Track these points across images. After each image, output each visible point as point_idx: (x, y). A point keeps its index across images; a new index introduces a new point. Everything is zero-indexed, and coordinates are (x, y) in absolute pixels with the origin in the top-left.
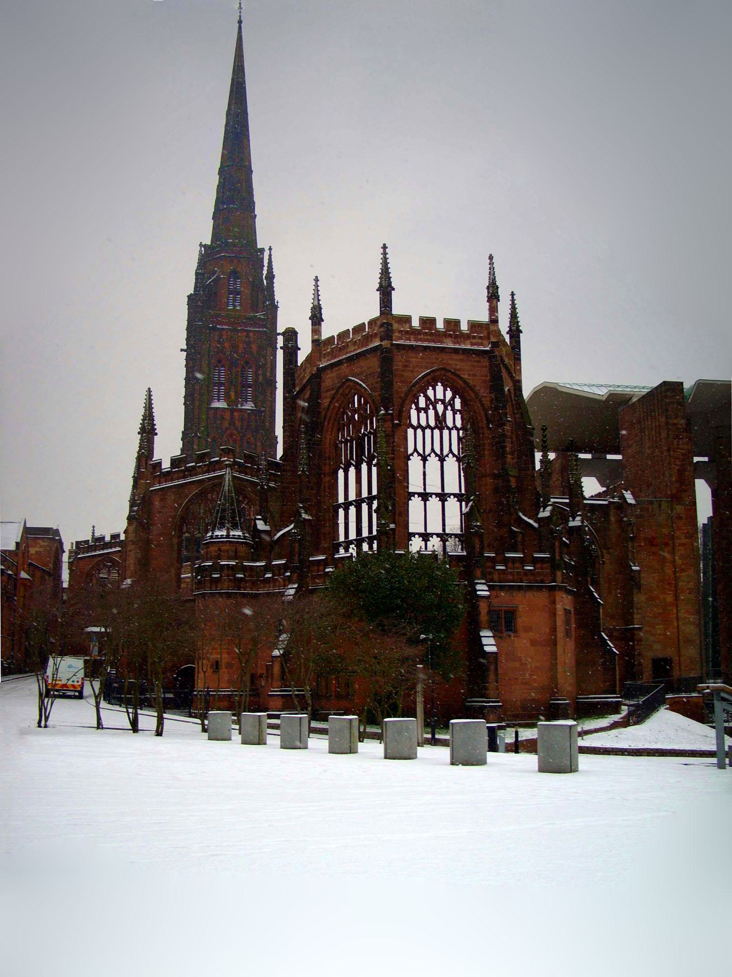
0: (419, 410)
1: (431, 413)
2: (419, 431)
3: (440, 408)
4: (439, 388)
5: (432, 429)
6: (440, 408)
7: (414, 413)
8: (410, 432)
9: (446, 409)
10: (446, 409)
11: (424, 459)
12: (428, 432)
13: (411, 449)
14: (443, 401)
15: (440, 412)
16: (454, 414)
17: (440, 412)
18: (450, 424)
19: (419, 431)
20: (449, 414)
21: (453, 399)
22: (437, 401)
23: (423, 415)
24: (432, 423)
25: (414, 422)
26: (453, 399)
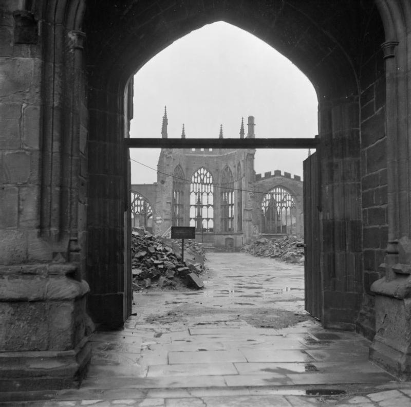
0: (195, 177)
1: (199, 178)
2: (195, 185)
3: (202, 176)
4: (202, 170)
5: (199, 184)
6: (202, 176)
7: (193, 178)
8: (192, 185)
9: (204, 177)
10: (204, 177)
11: (196, 194)
12: (197, 185)
13: (191, 190)
14: (203, 174)
15: (202, 178)
16: (207, 178)
17: (202, 178)
18: (205, 182)
19: (195, 185)
20: (205, 178)
21: (206, 174)
22: (201, 174)
23: (196, 179)
24: (199, 182)
25: (193, 181)
26: (206, 174)
